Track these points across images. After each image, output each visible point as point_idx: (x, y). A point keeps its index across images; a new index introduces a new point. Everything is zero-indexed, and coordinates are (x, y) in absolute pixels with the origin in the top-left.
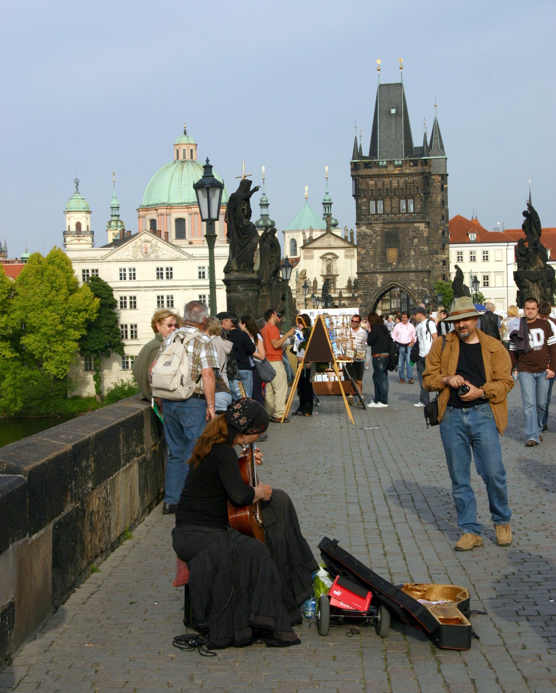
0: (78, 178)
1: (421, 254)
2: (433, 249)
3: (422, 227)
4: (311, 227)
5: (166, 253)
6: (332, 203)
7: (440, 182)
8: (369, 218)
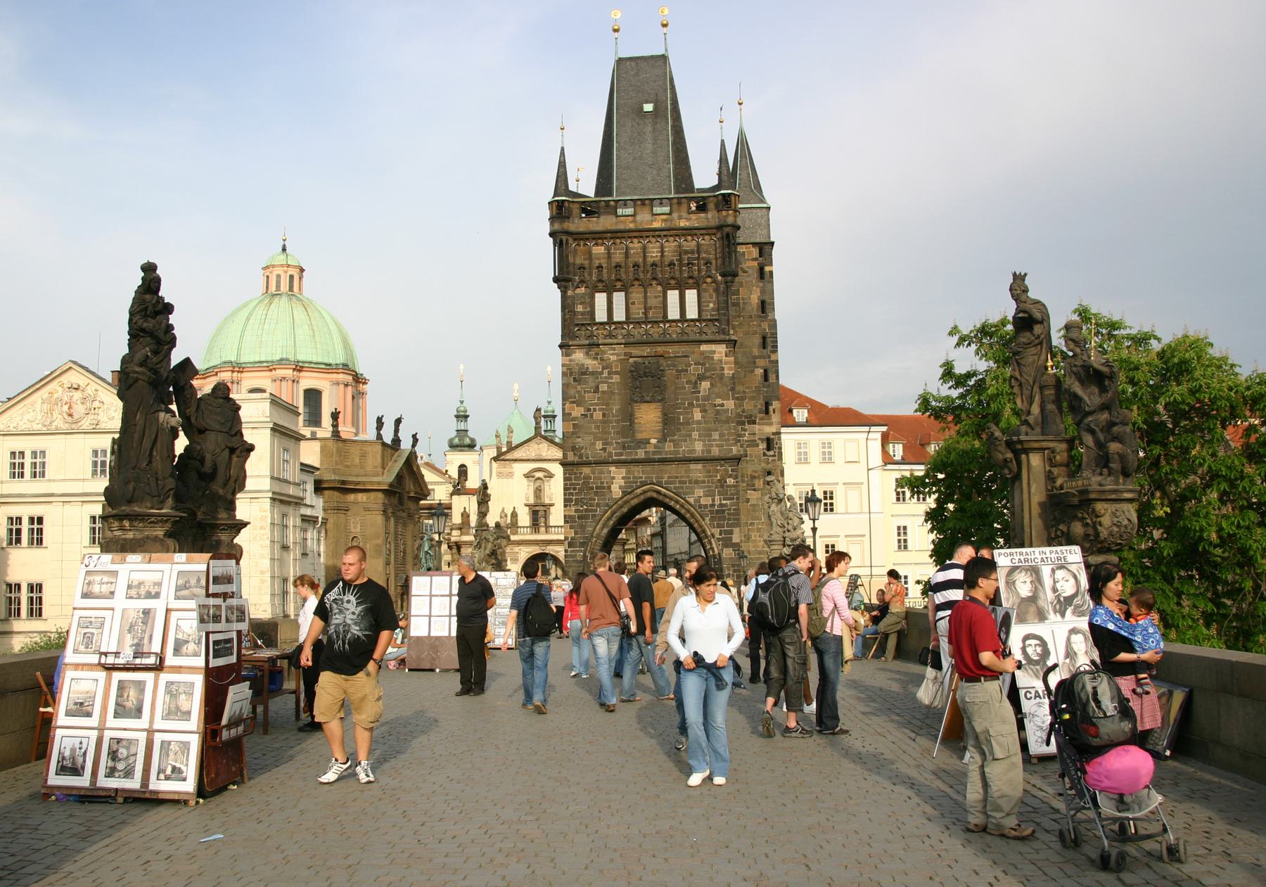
1: (719, 417)
2: (743, 412)
3: (720, 353)
4: (509, 426)
7: (756, 259)
8: (592, 332)
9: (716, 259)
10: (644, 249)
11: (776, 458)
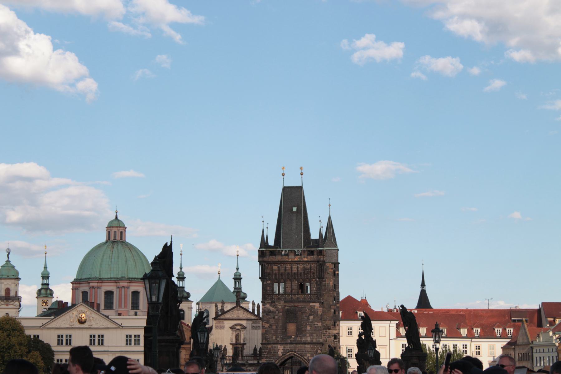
0: (9, 248)
1: (316, 329)
3: (317, 306)
4: (222, 301)
5: (98, 322)
6: (242, 278)
7: (332, 269)
11: (337, 342)
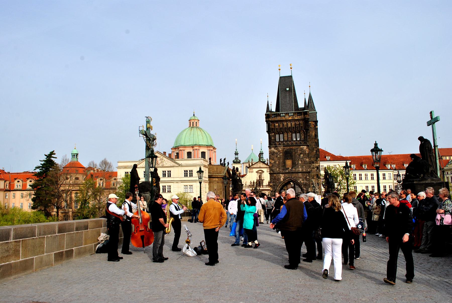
1: (305, 163)
3: (305, 148)
5: (167, 163)
7: (313, 125)
9: (304, 126)
10: (287, 124)
11: (319, 171)
